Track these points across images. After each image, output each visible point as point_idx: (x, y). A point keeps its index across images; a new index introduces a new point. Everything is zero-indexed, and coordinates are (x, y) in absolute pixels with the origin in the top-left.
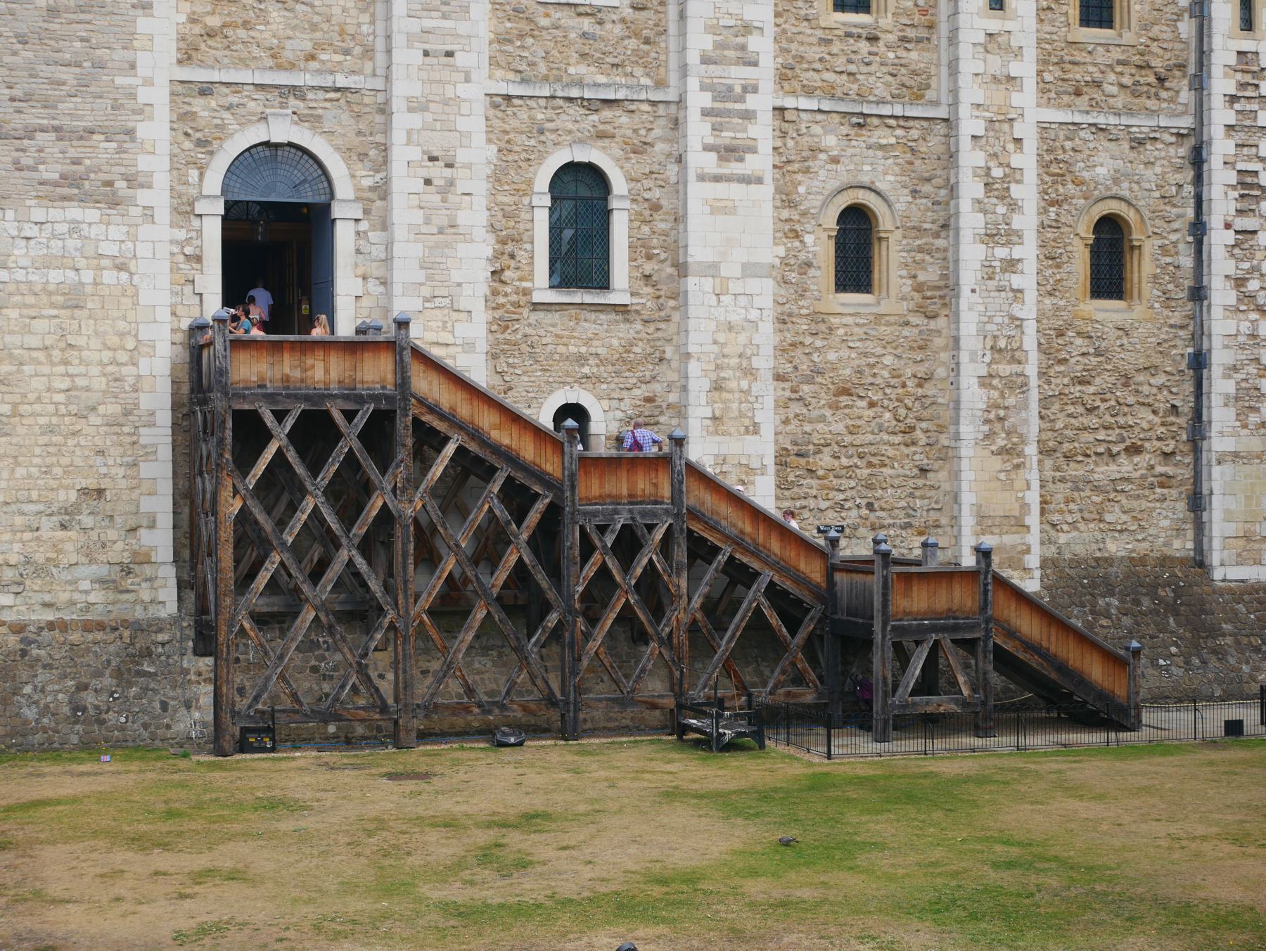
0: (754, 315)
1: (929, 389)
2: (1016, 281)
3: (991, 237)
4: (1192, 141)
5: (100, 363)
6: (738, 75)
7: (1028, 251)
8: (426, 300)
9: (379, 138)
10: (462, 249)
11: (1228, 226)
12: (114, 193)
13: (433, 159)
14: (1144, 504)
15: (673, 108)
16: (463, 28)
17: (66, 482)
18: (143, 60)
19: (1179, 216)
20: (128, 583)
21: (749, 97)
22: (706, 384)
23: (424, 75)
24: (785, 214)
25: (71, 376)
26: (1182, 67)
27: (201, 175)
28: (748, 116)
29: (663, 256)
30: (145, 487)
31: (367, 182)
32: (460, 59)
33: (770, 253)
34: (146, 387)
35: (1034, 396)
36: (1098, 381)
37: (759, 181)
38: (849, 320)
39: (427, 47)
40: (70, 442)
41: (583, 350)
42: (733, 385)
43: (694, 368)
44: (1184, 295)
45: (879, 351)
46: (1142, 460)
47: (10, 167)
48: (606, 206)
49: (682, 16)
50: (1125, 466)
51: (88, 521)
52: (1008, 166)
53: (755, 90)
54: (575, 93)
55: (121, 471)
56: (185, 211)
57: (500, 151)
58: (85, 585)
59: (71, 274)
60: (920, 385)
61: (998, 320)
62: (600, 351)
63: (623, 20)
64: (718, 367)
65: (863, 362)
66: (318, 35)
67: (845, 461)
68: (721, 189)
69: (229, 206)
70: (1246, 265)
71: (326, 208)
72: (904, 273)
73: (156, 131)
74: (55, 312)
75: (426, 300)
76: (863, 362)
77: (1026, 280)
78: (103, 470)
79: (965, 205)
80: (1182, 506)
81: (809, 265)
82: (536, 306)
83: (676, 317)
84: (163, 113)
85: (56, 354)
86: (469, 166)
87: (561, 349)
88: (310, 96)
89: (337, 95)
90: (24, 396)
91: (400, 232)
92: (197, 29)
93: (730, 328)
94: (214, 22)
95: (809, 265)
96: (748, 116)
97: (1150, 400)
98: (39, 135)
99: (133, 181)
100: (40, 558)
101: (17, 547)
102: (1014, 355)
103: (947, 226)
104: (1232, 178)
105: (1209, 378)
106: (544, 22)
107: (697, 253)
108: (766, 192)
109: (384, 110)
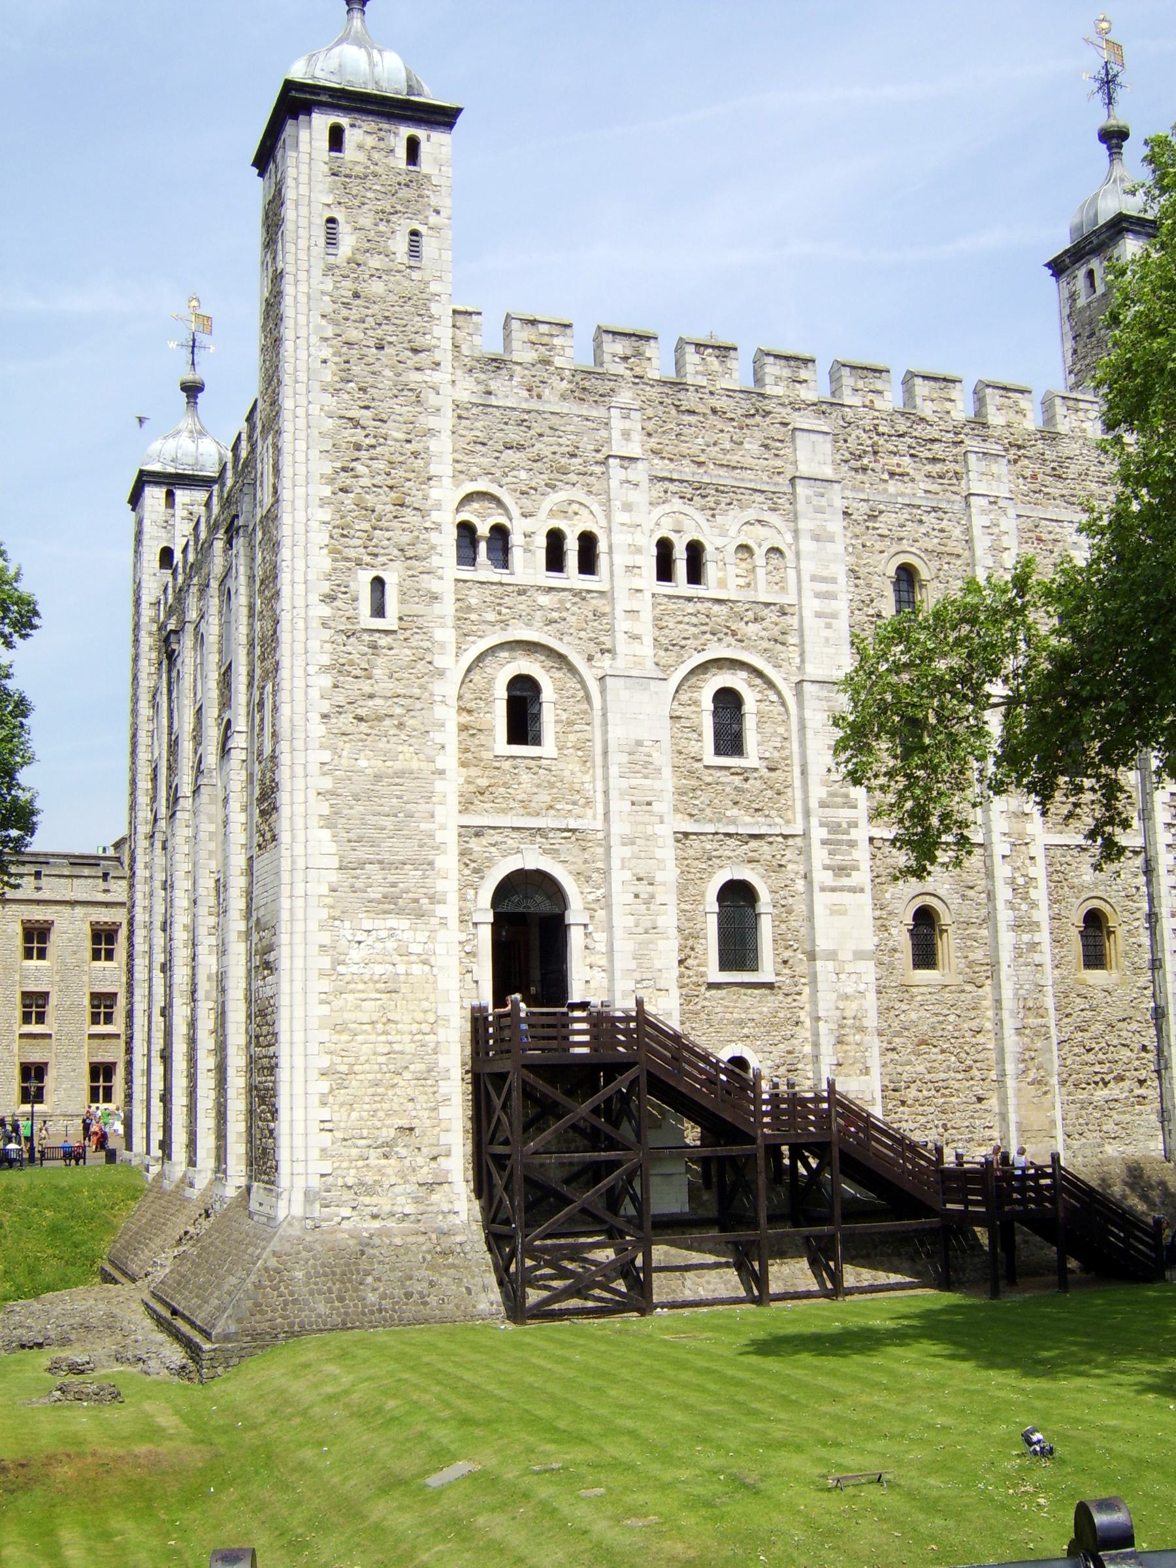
0: (862, 987)
1: (980, 1038)
2: (1037, 958)
3: (1017, 926)
5: (411, 1033)
6: (844, 814)
7: (1044, 937)
8: (638, 982)
9: (600, 865)
10: (662, 944)
13: (639, 879)
14: (1128, 1118)
15: (798, 840)
16: (658, 785)
17: (387, 1122)
18: (439, 811)
20: (435, 1197)
21: (852, 830)
22: (833, 1041)
23: (632, 818)
24: (878, 913)
28: (852, 844)
30: (444, 1125)
31: (591, 897)
33: (869, 942)
35: (1055, 1041)
37: (862, 890)
40: (390, 1093)
42: (850, 1039)
45: (946, 1012)
46: (1126, 1084)
49: (804, 773)
50: (1114, 1091)
51: (403, 1152)
53: (856, 826)
55: (426, 1114)
58: (401, 1200)
59: (391, 967)
64: (841, 1027)
65: (935, 1019)
67: (925, 1093)
68: (836, 897)
69: (496, 915)
71: (561, 917)
73: (448, 862)
74: (378, 996)
75: (638, 982)
76: (935, 1019)
77: (1045, 956)
78: (414, 1113)
79: (1000, 905)
80: (1154, 1117)
82: (711, 986)
84: (453, 849)
85: (380, 1026)
86: (664, 884)
87: (728, 1016)
91: (618, 933)
92: (472, 788)
93: (846, 997)
94: (484, 782)
96: (852, 844)
99: (432, 899)
100: (369, 1180)
101: (353, 1172)
103: (990, 919)
106: (709, 779)
107: (823, 943)
108: (866, 899)
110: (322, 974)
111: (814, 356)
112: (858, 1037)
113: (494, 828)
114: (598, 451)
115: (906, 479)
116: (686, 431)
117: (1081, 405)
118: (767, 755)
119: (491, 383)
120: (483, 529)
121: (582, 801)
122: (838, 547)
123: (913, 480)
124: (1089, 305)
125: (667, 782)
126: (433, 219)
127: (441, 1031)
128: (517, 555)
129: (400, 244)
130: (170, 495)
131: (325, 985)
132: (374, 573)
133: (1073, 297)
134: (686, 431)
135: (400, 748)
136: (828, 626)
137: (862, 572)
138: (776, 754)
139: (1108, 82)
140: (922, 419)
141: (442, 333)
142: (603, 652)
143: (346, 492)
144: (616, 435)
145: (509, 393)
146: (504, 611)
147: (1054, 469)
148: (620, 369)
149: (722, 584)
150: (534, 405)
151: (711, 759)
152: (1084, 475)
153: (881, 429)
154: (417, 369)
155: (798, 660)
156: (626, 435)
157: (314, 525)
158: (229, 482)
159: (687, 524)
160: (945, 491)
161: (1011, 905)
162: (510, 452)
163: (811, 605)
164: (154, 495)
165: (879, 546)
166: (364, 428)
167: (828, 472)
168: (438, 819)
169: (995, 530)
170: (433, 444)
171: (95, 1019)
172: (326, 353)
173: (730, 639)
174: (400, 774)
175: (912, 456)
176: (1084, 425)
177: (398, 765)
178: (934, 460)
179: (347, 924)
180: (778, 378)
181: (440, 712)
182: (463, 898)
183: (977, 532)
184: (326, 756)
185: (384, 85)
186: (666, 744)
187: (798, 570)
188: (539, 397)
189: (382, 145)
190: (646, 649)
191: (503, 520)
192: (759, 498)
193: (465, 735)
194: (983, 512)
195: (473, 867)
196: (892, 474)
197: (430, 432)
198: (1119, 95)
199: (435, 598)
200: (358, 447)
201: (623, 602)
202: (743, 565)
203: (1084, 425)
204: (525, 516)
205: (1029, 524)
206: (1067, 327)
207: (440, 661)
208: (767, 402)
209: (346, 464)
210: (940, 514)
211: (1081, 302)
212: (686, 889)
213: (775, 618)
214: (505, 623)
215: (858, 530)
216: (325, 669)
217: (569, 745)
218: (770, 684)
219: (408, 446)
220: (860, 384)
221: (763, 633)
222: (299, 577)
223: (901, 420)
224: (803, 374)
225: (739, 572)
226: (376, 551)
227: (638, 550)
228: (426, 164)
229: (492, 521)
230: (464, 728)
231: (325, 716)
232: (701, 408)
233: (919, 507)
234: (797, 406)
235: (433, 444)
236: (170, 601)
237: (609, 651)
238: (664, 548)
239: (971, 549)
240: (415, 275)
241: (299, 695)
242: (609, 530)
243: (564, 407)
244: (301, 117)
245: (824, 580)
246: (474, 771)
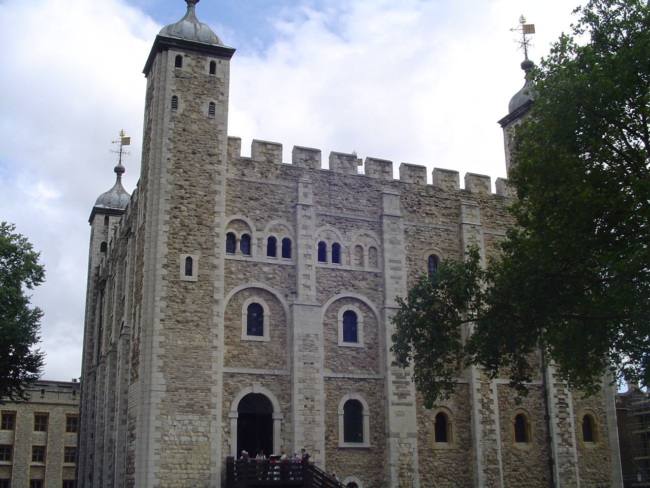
0: (412, 450)
2: (494, 437)
3: (484, 422)
4: (543, 389)
5: (198, 469)
7: (497, 427)
9: (288, 392)
10: (317, 429)
11: (557, 417)
12: (204, 411)
15: (382, 381)
16: (316, 355)
18: (214, 365)
19: (541, 414)
22: (397, 476)
24: (419, 416)
25: (188, 474)
26: (538, 365)
27: (231, 405)
28: (407, 383)
29: (380, 431)
31: (284, 407)
32: (316, 365)
33: (415, 429)
34: (213, 478)
36: (520, 470)
37: (411, 405)
38: (441, 452)
39: (305, 361)
41: (355, 463)
42: (406, 474)
43: (393, 469)
44: (544, 440)
47: (170, 401)
48: (361, 414)
52: (489, 398)
54: (351, 376)
56: (225, 417)
57: (327, 395)
60: (464, 473)
61: (489, 450)
62: (361, 464)
63: (365, 352)
64: (401, 469)
66: (269, 357)
68: (399, 408)
70: (564, 429)
72: (457, 435)
73: (218, 389)
77: (497, 436)
79: (476, 412)
81: (427, 433)
83: (385, 452)
85: (183, 466)
86: (319, 401)
87: (348, 463)
88: (266, 377)
89: (275, 377)
90: (172, 480)
91: (297, 424)
92: (230, 355)
93: (404, 455)
94: (235, 352)
95: (427, 433)
96: (407, 383)
97: (537, 476)
98: (180, 390)
102: (495, 462)
103: (469, 419)
104: (556, 400)
105: (555, 468)
106: (341, 353)
108: (413, 409)
109: (290, 382)
110: (157, 441)
111: (241, 137)
112: (409, 474)
113: (240, 374)
114: (292, 202)
115: (434, 216)
116: (333, 193)
118: (368, 342)
119: (245, 170)
120: (239, 236)
121: (281, 362)
122: (402, 246)
123: (436, 217)
125: (321, 353)
126: (221, 97)
127: (212, 469)
128: (254, 249)
129: (205, 109)
130: (107, 219)
131: (158, 446)
132: (188, 255)
134: (333, 193)
135: (197, 336)
136: (397, 283)
137: (413, 258)
138: (372, 341)
139: (525, 44)
141: (223, 148)
142: (292, 293)
143: (176, 218)
144: (301, 194)
145: (253, 176)
146: (247, 274)
147: (501, 212)
148: (304, 165)
149: (349, 263)
150: (263, 180)
151: (341, 343)
153: (422, 194)
154: (210, 163)
155: (382, 298)
156: (306, 195)
157: (161, 233)
158: (129, 213)
159: (332, 235)
160: (451, 222)
161: (481, 412)
162: (252, 201)
163: (388, 273)
164: (100, 218)
166: (185, 189)
167: (398, 213)
168: (214, 369)
169: (474, 240)
170: (217, 198)
171: (34, 459)
172: (170, 156)
173: (351, 288)
174: (194, 348)
175: (436, 206)
177: (196, 344)
179: (169, 417)
180: (375, 171)
181: (216, 319)
182: (224, 406)
184: (162, 339)
185: (201, 39)
186: (321, 336)
187: (383, 257)
188: (266, 177)
189: (199, 65)
190: (313, 293)
191: (247, 232)
192: (366, 224)
193: (227, 330)
194: (469, 232)
195: (230, 392)
196: (427, 214)
197: (215, 192)
198: (529, 49)
199: (215, 267)
200: (182, 198)
201: (302, 271)
202: (358, 254)
204: (257, 230)
206: (508, 150)
207: (216, 296)
208: (371, 181)
209: (176, 206)
212: (330, 403)
213: (372, 279)
214: (247, 280)
215: (411, 239)
216: (163, 298)
217: (276, 336)
218: (370, 309)
219: (205, 198)
220: (413, 174)
221: (367, 286)
222: (152, 256)
224: (387, 169)
225: (356, 258)
226: (189, 245)
227: (310, 247)
228: (218, 74)
229: (243, 233)
230: (226, 327)
231: (162, 320)
232: (340, 183)
233: (439, 229)
234: (384, 183)
235: (217, 198)
236: (104, 266)
237: (295, 293)
238: (322, 246)
240: (211, 122)
241: (149, 310)
242: (296, 237)
243: (278, 182)
244: (163, 52)
245: (395, 261)
246: (231, 347)
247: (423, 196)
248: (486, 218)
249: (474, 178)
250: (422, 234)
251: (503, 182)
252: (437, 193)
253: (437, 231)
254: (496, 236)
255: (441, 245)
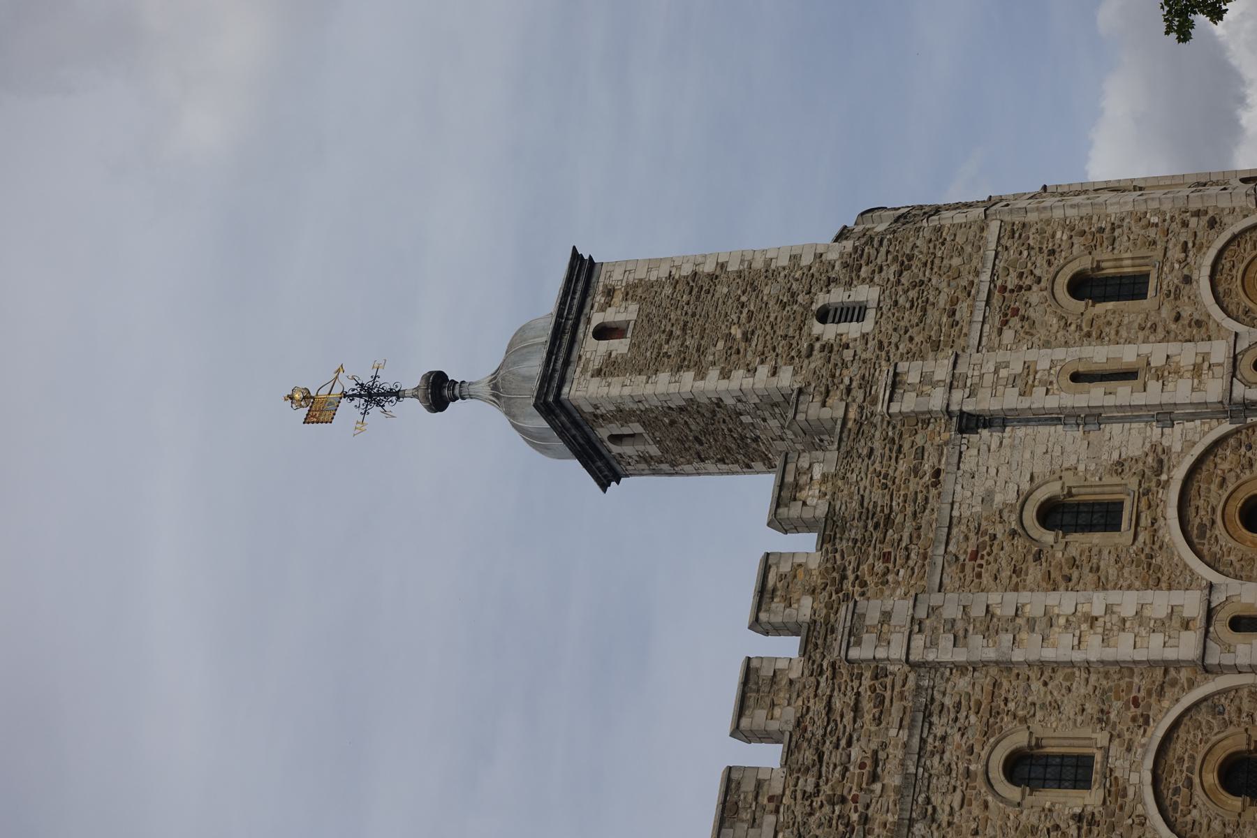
115: (882, 755)
117: (790, 479)
123: (884, 746)
124: (656, 442)
133: (645, 459)
139: (370, 395)
140: (798, 723)
147: (876, 526)
152: (887, 483)
153: (810, 788)
160: (902, 697)
165: (976, 810)
169: (960, 625)
175: (849, 744)
176: (817, 475)
178: (856, 709)
183: (961, 656)
194: (933, 644)
196: (874, 777)
198: (387, 381)
203: (817, 475)
205: (952, 570)
206: (687, 468)
210: (935, 708)
211: (654, 450)
223: (799, 757)
233: (923, 741)
239: (985, 664)
247: (817, 785)
248: (890, 577)
249: (764, 607)
250: (936, 799)
251: (783, 511)
252: (808, 735)
253: (929, 748)
254: (952, 548)
255: (974, 736)
